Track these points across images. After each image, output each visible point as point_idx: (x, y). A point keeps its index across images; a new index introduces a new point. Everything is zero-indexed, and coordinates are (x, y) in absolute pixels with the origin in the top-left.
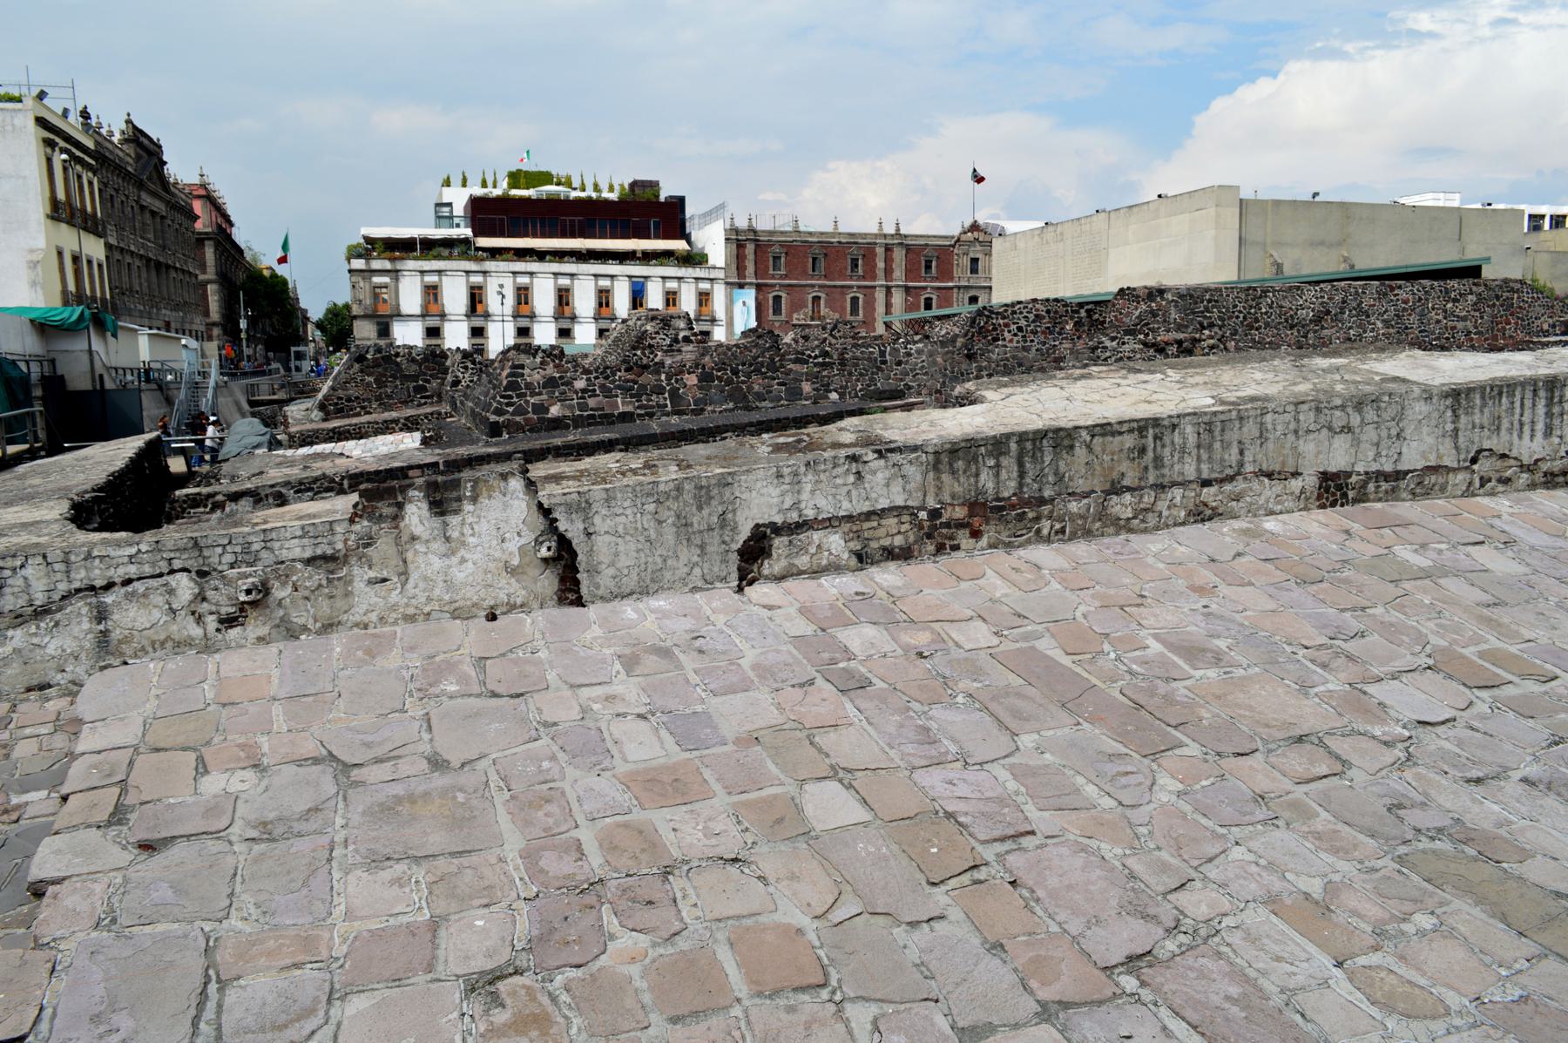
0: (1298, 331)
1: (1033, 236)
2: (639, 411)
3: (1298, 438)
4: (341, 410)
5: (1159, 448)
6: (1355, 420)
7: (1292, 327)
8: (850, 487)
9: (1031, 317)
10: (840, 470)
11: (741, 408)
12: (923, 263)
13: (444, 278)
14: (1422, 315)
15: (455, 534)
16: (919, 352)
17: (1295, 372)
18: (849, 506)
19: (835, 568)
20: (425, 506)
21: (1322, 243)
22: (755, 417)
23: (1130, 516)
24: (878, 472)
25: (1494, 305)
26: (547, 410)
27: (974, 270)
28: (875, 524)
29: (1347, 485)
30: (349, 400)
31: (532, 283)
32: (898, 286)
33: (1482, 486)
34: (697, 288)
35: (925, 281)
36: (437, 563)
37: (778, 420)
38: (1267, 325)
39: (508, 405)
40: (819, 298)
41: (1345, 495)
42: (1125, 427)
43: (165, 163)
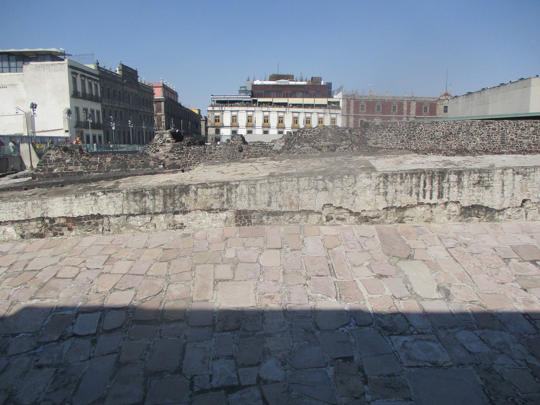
0: (435, 141)
3: (299, 192)
5: (229, 194)
7: (432, 139)
8: (93, 205)
14: (503, 135)
26: (53, 170)
27: (446, 111)
29: (251, 217)
33: (327, 221)
34: (330, 117)
35: (424, 115)
41: (250, 221)
42: (213, 185)
43: (138, 77)
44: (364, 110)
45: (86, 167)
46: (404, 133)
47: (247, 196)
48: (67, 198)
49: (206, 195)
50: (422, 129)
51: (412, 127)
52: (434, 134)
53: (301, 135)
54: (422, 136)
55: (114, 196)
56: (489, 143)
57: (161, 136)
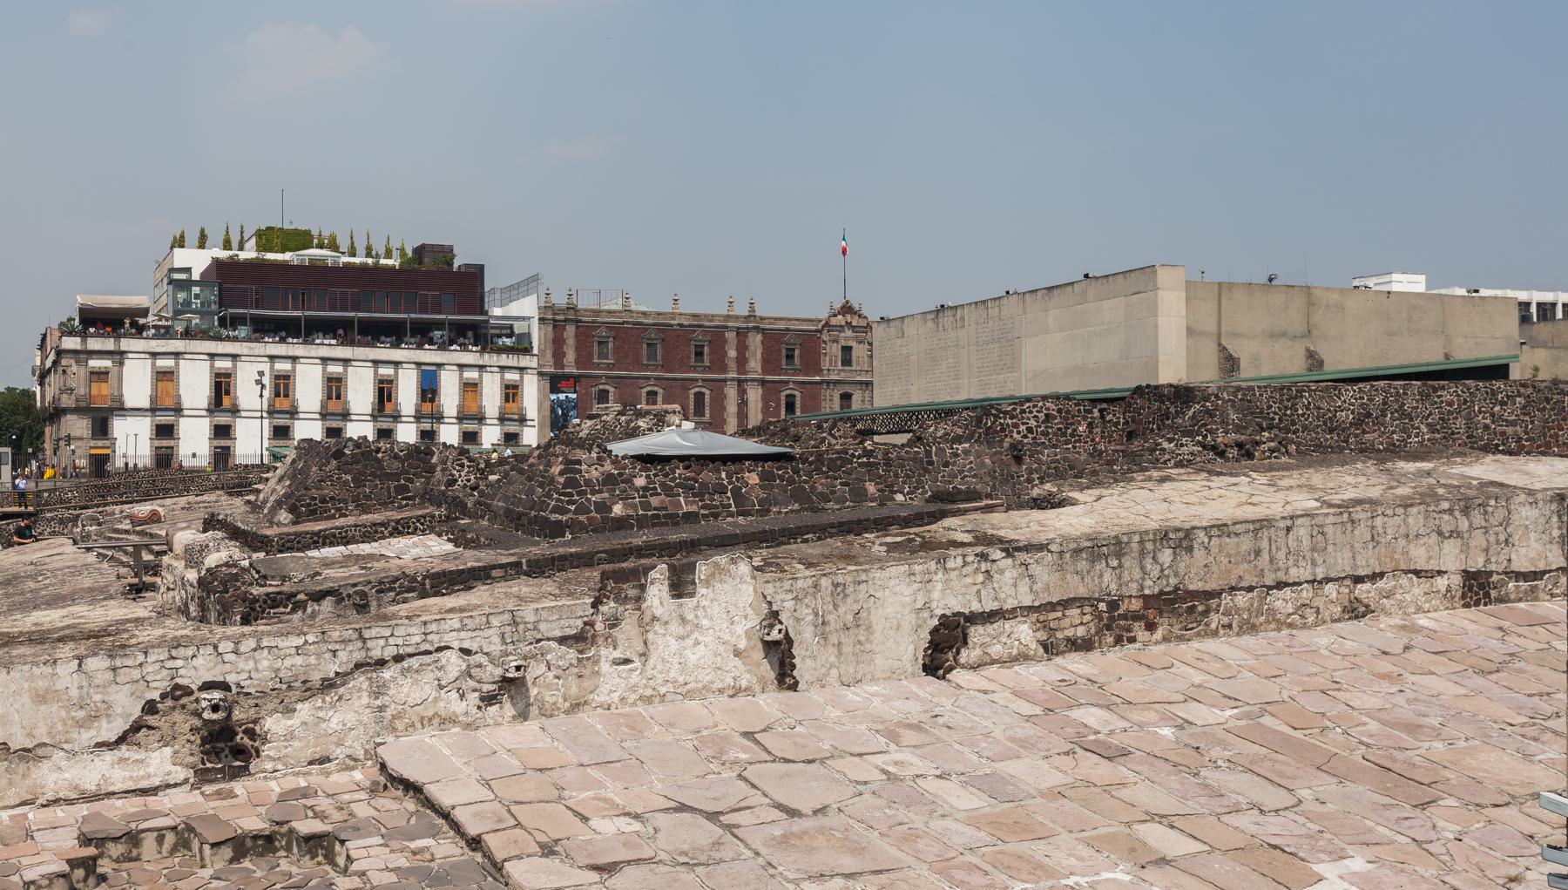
0: (1338, 435)
1: (926, 321)
2: (702, 512)
4: (313, 512)
6: (1464, 524)
7: (1331, 431)
9: (1042, 416)
10: (969, 569)
11: (806, 509)
12: (784, 352)
13: (182, 362)
14: (1469, 419)
15: (690, 617)
16: (966, 452)
17: (1384, 479)
18: (979, 606)
19: (1023, 657)
20: (666, 588)
21: (1284, 335)
22: (823, 519)
23: (1291, 611)
24: (1007, 570)
25: (1544, 408)
26: (610, 510)
27: (847, 361)
28: (1059, 614)
29: (1489, 584)
30: (323, 501)
31: (294, 370)
32: (753, 380)
34: (502, 379)
36: (674, 645)
37: (859, 522)
38: (1305, 428)
39: (570, 502)
40: (655, 393)
41: (1487, 595)
44: (607, 359)
45: (701, 501)
46: (1271, 415)
47: (1308, 555)
48: (917, 568)
49: (1229, 555)
50: (1309, 403)
51: (1288, 400)
52: (1335, 416)
53: (993, 423)
54: (1311, 423)
55: (1032, 561)
56: (1445, 437)
57: (659, 420)
